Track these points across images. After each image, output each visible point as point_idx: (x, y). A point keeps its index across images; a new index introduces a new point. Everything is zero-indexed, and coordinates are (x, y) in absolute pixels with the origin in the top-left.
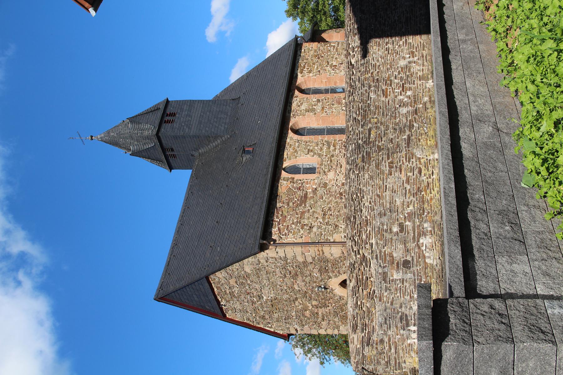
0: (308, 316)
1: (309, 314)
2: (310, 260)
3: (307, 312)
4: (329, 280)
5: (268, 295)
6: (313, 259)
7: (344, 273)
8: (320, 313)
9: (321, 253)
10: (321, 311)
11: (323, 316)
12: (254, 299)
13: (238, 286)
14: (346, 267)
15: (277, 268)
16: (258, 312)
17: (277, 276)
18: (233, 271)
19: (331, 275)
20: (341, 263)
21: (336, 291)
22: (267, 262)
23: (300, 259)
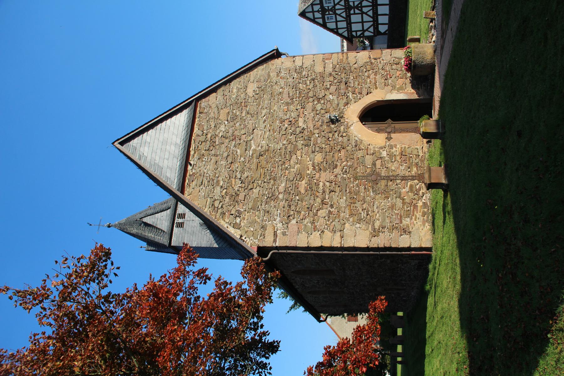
0: (303, 191)
1: (305, 187)
2: (329, 69)
3: (304, 182)
4: (346, 107)
5: (259, 140)
6: (334, 68)
7: (368, 94)
8: (321, 184)
9: (344, 59)
10: (325, 176)
11: (324, 192)
12: (238, 151)
13: (226, 122)
14: (370, 81)
15: (287, 86)
16: (233, 183)
17: (282, 102)
18: (232, 92)
19: (351, 97)
20: (366, 74)
21: (352, 128)
22: (278, 76)
23: (319, 69)
